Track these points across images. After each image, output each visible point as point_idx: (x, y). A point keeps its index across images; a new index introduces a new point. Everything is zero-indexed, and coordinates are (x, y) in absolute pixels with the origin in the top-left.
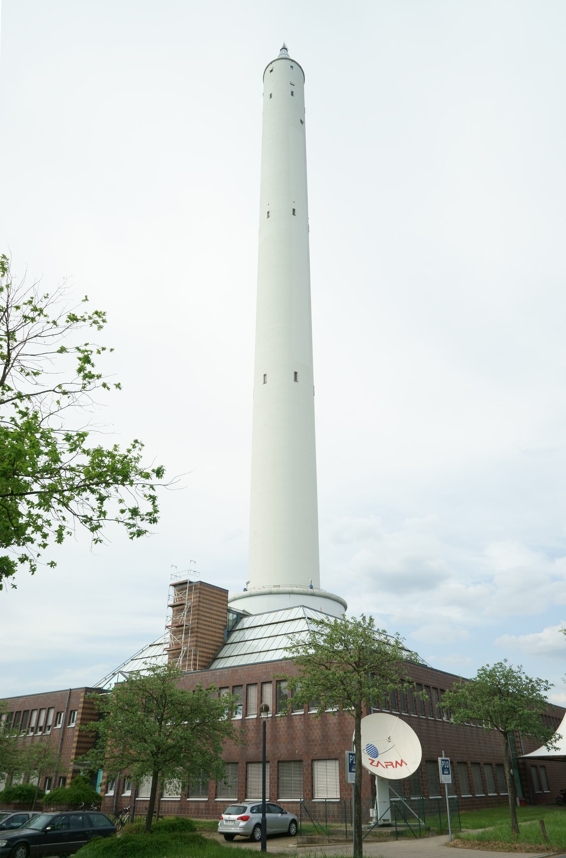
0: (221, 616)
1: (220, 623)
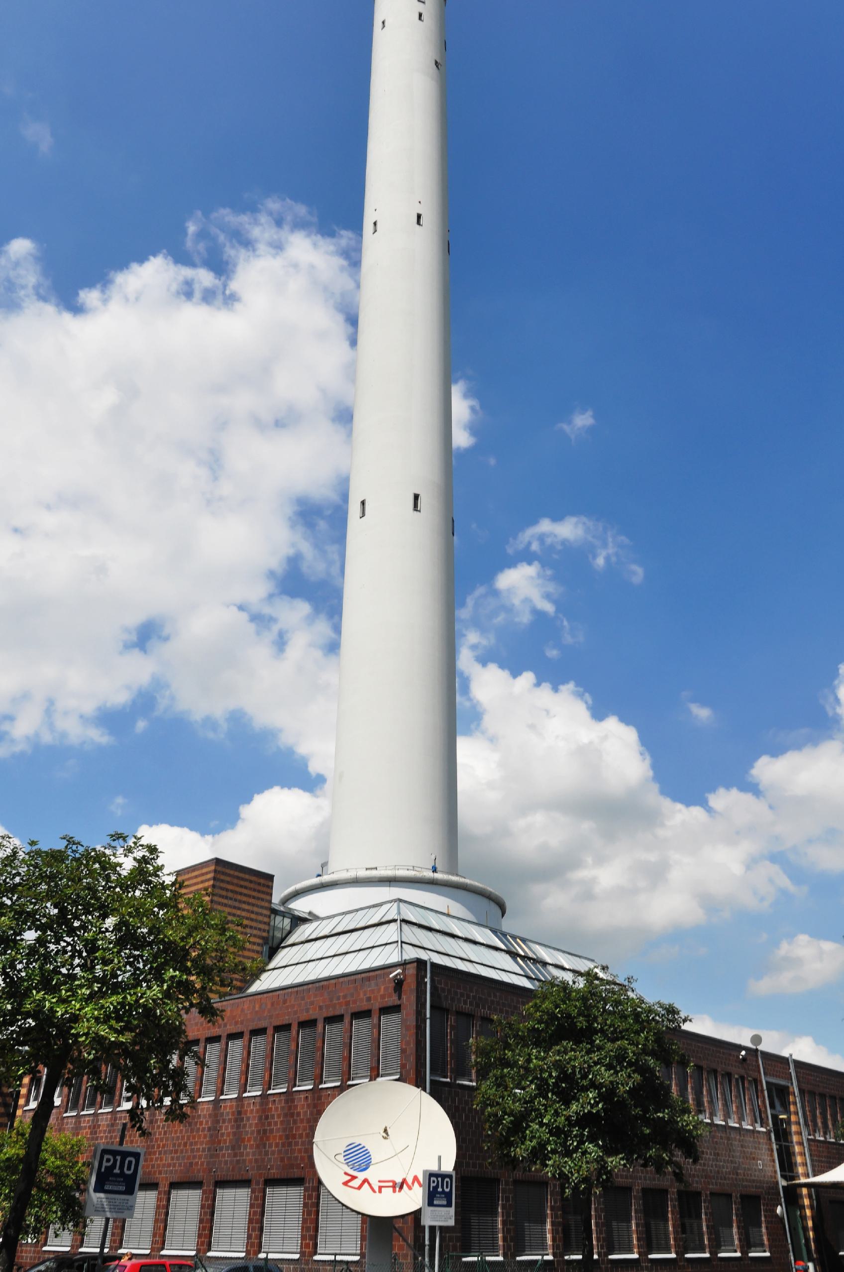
0: (256, 921)
1: (255, 932)
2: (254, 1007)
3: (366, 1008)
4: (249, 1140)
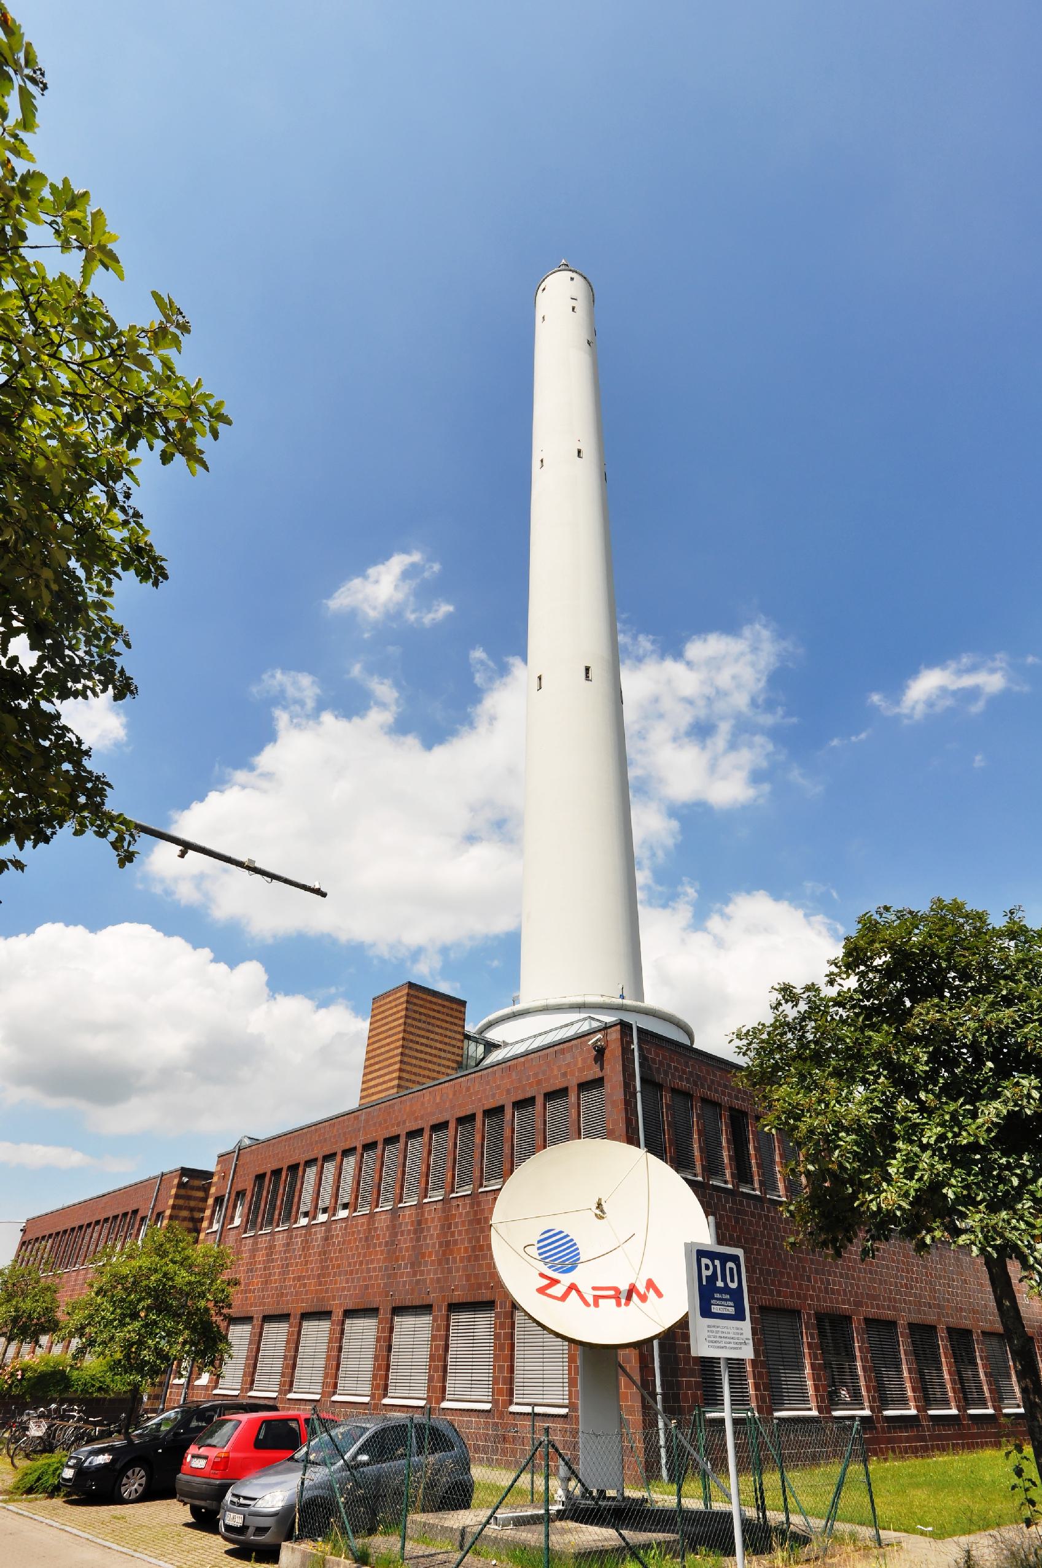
0: (449, 1045)
1: (449, 1056)
2: (435, 1098)
4: (430, 1255)
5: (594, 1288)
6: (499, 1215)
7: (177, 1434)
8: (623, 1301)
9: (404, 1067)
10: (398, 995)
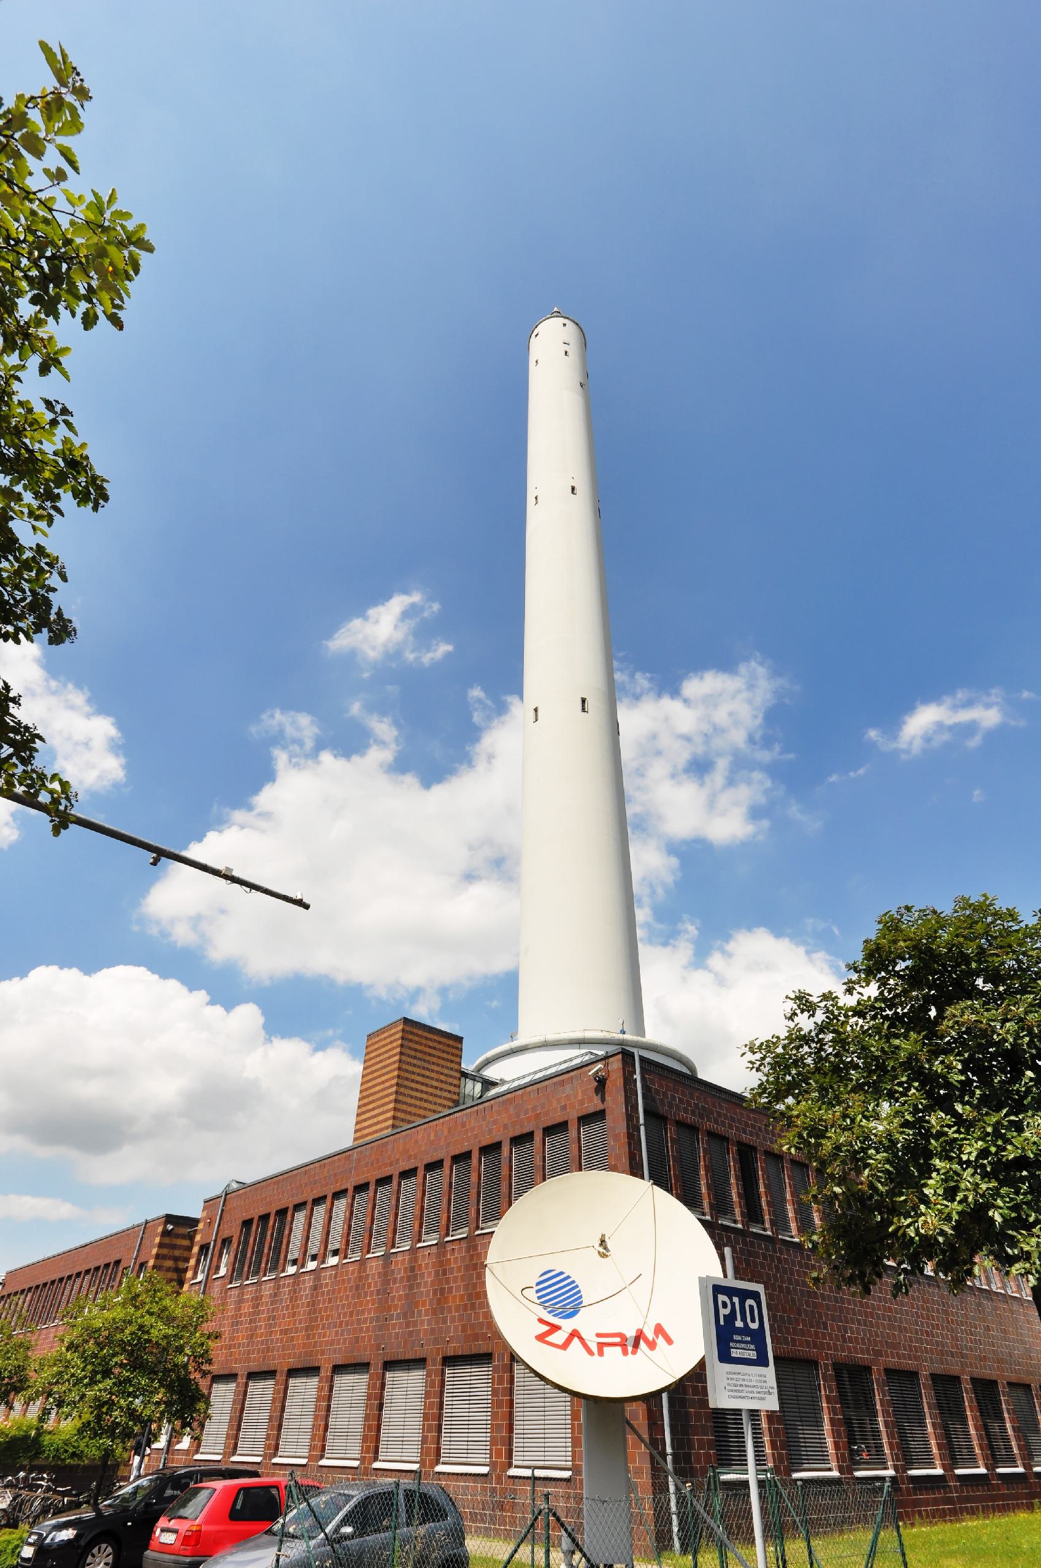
0: (446, 1083)
2: (429, 1136)
3: (561, 1120)
4: (424, 1304)
5: (598, 1335)
6: (494, 1255)
7: (148, 1505)
8: (630, 1349)
9: (399, 1106)
10: (393, 1031)
